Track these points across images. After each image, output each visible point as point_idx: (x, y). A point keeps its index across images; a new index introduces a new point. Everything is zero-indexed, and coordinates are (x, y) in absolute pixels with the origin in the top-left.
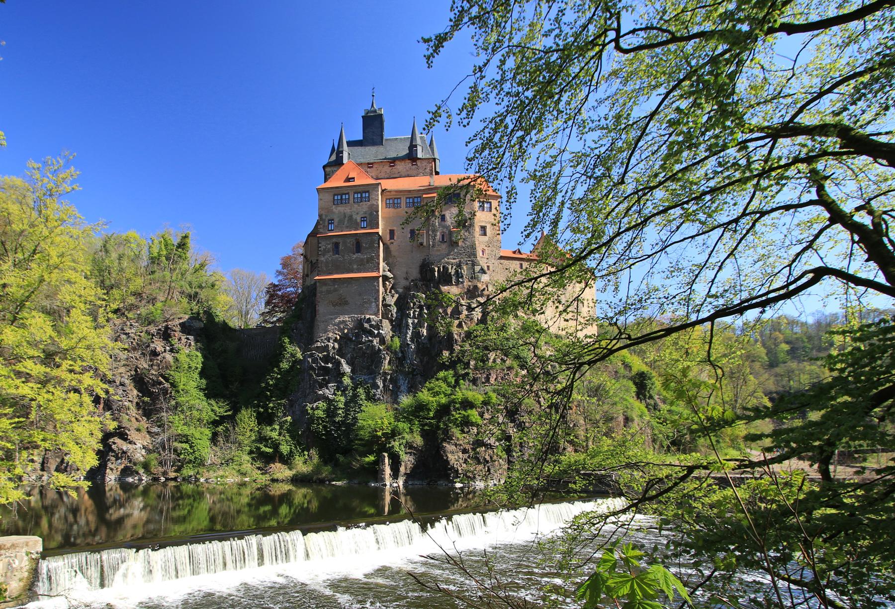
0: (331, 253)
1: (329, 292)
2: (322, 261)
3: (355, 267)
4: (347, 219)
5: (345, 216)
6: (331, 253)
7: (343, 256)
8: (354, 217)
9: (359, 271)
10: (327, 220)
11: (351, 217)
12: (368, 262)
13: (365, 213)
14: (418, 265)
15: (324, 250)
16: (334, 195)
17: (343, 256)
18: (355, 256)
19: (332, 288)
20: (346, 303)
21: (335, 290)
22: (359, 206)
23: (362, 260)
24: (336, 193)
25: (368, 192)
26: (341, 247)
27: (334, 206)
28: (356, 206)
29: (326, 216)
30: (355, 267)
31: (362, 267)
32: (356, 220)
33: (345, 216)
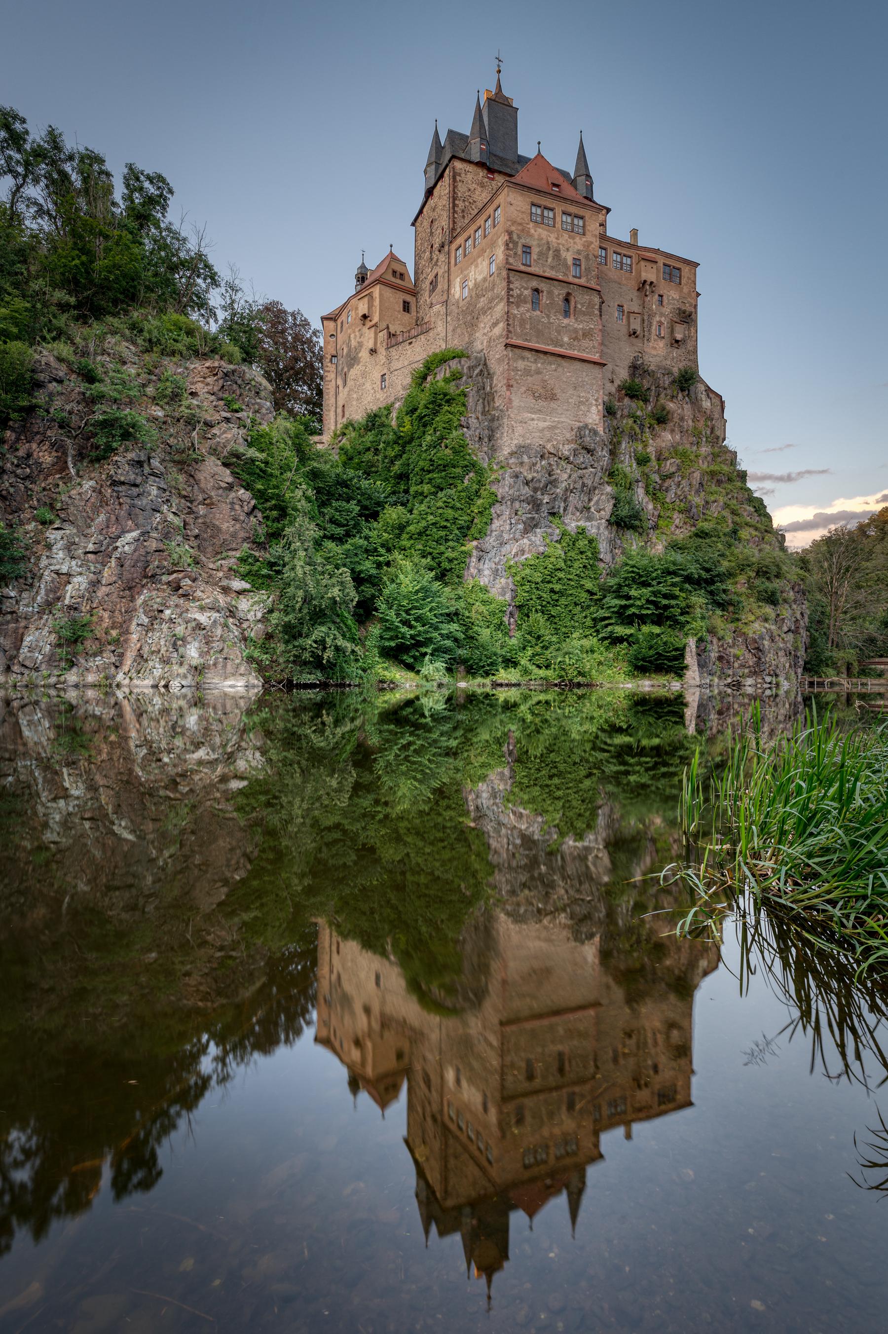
0: (529, 306)
1: (527, 372)
2: (515, 316)
3: (566, 339)
7: (548, 317)
8: (564, 254)
9: (571, 346)
11: (557, 251)
13: (579, 252)
14: (627, 363)
15: (519, 296)
17: (548, 317)
20: (553, 397)
21: (538, 372)
22: (570, 237)
23: (576, 331)
26: (544, 299)
27: (531, 225)
29: (519, 237)
31: (575, 343)
32: (565, 259)
33: (549, 249)
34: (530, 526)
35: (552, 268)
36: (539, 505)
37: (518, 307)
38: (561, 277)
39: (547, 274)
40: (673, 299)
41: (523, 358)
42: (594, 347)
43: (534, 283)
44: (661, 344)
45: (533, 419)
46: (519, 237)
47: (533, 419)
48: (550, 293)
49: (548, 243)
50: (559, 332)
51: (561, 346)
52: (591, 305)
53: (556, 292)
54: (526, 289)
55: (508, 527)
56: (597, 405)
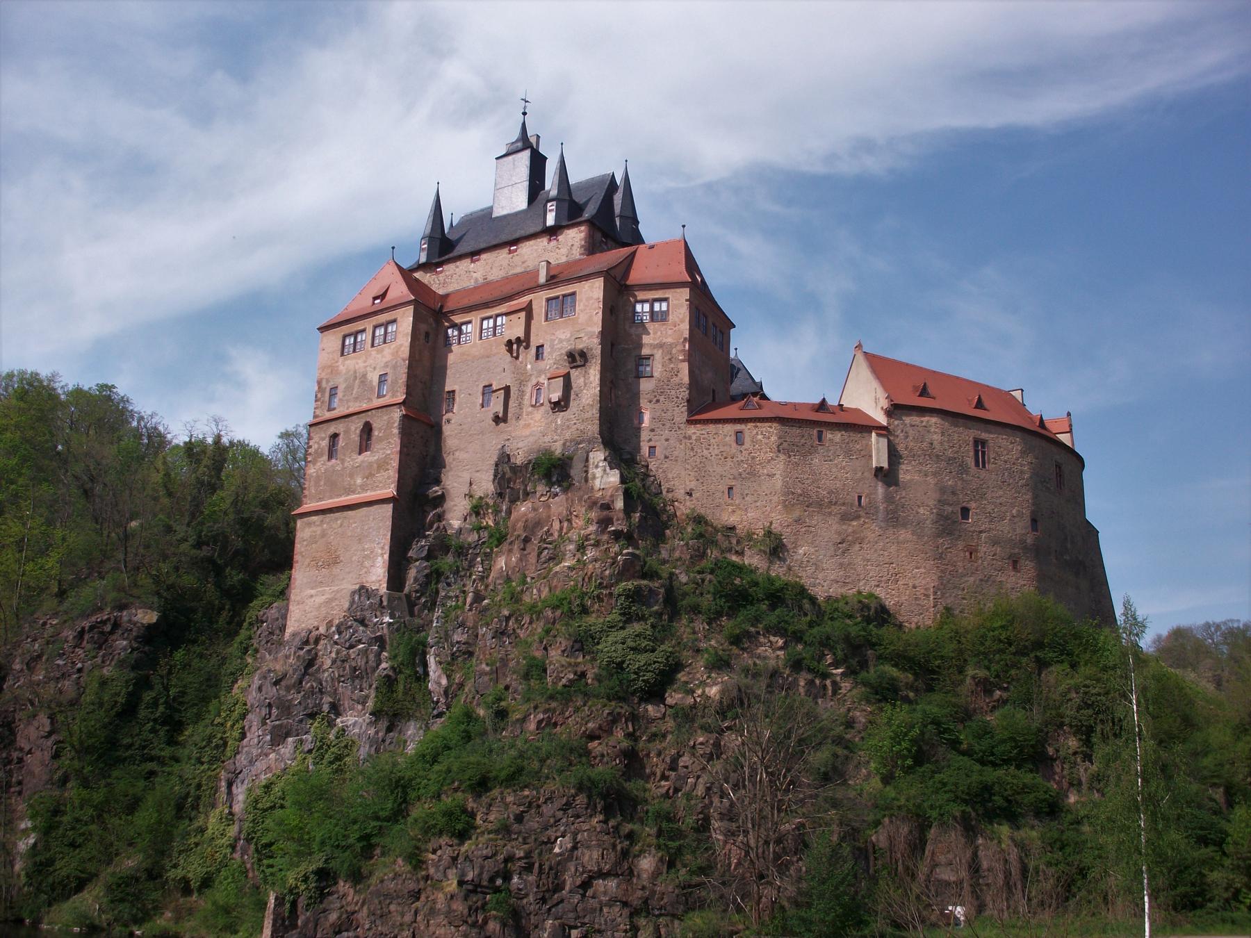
2: (311, 475)
3: (359, 481)
4: (357, 381)
5: (356, 377)
6: (325, 457)
7: (343, 461)
8: (370, 376)
9: (364, 488)
10: (328, 390)
12: (379, 467)
13: (386, 366)
15: (316, 451)
16: (345, 337)
18: (361, 458)
19: (318, 530)
20: (335, 561)
24: (347, 332)
25: (394, 321)
28: (373, 352)
30: (359, 481)
32: (371, 381)
34: (279, 737)
35: (356, 399)
36: (289, 708)
37: (314, 464)
38: (365, 406)
39: (351, 410)
40: (561, 341)
41: (309, 524)
42: (389, 478)
43: (332, 429)
44: (539, 415)
45: (312, 596)
46: (328, 381)
47: (312, 596)
48: (347, 432)
49: (355, 372)
50: (351, 476)
51: (354, 492)
52: (389, 425)
53: (353, 428)
54: (323, 439)
55: (256, 740)
56: (382, 555)
